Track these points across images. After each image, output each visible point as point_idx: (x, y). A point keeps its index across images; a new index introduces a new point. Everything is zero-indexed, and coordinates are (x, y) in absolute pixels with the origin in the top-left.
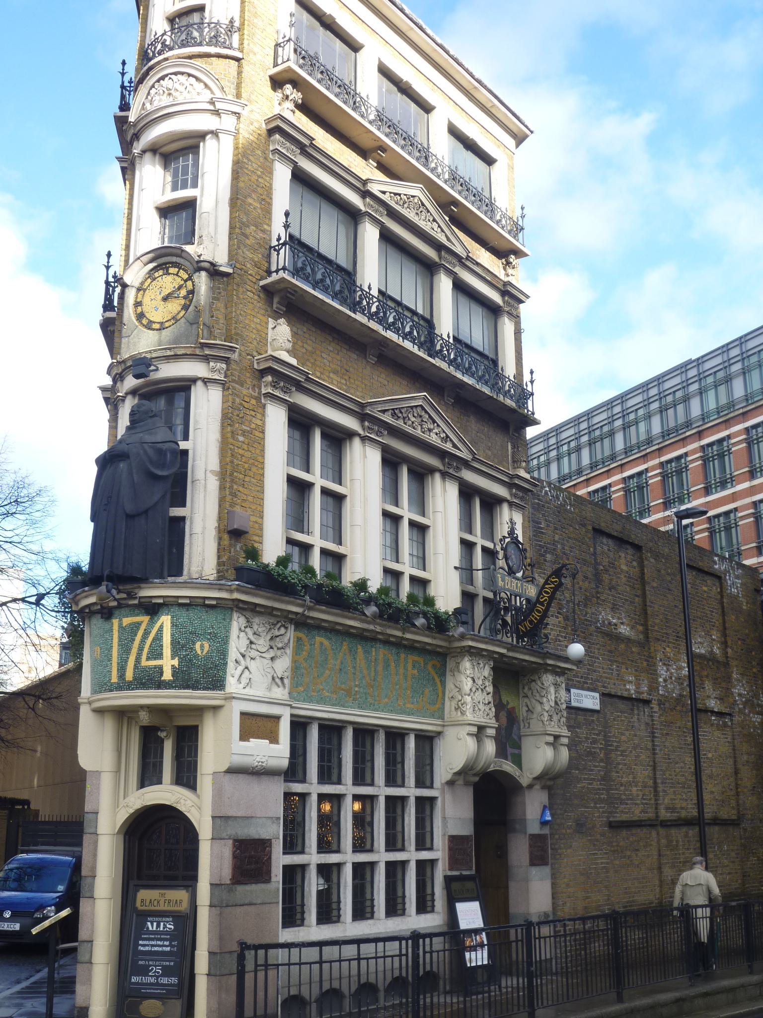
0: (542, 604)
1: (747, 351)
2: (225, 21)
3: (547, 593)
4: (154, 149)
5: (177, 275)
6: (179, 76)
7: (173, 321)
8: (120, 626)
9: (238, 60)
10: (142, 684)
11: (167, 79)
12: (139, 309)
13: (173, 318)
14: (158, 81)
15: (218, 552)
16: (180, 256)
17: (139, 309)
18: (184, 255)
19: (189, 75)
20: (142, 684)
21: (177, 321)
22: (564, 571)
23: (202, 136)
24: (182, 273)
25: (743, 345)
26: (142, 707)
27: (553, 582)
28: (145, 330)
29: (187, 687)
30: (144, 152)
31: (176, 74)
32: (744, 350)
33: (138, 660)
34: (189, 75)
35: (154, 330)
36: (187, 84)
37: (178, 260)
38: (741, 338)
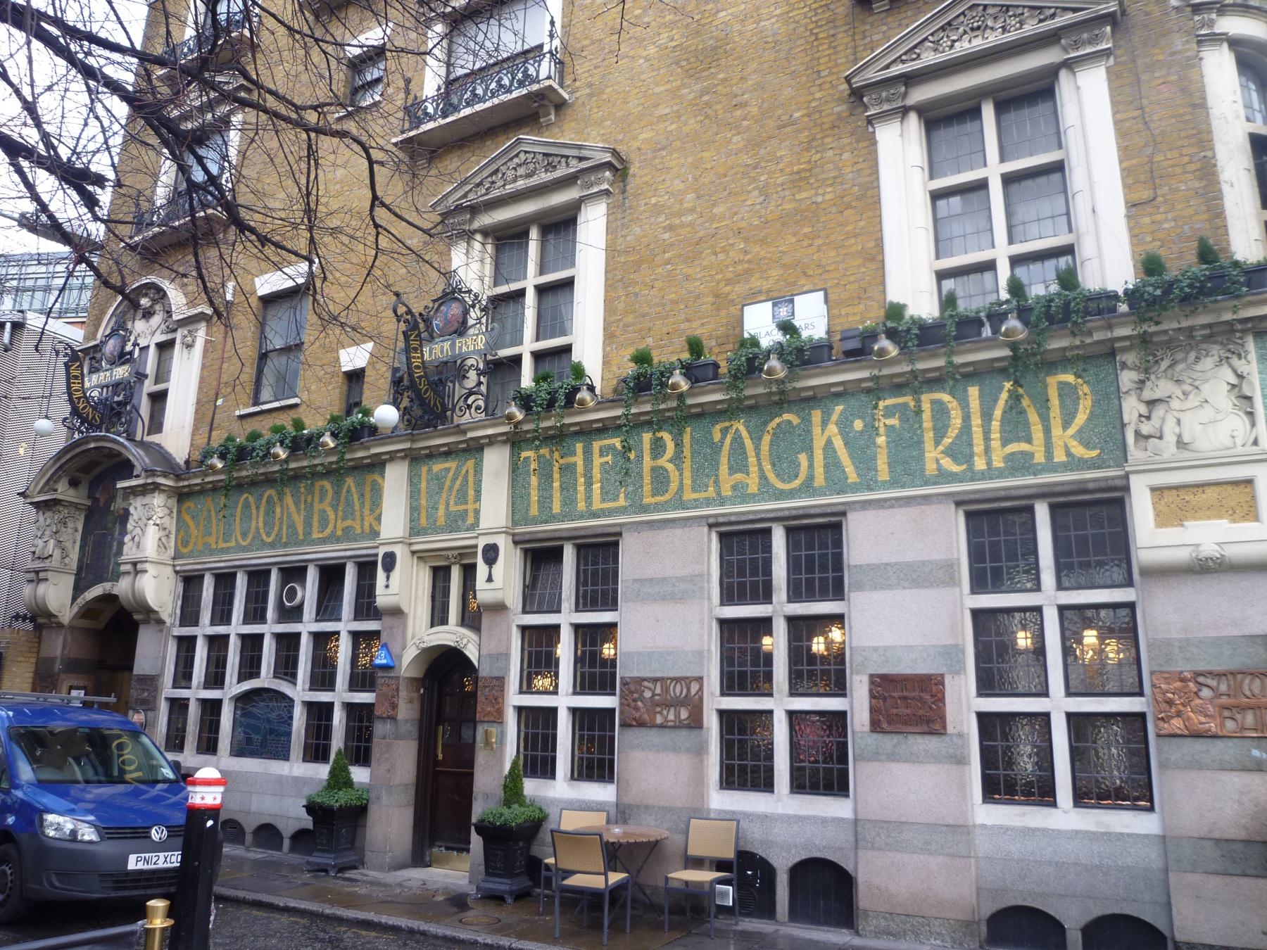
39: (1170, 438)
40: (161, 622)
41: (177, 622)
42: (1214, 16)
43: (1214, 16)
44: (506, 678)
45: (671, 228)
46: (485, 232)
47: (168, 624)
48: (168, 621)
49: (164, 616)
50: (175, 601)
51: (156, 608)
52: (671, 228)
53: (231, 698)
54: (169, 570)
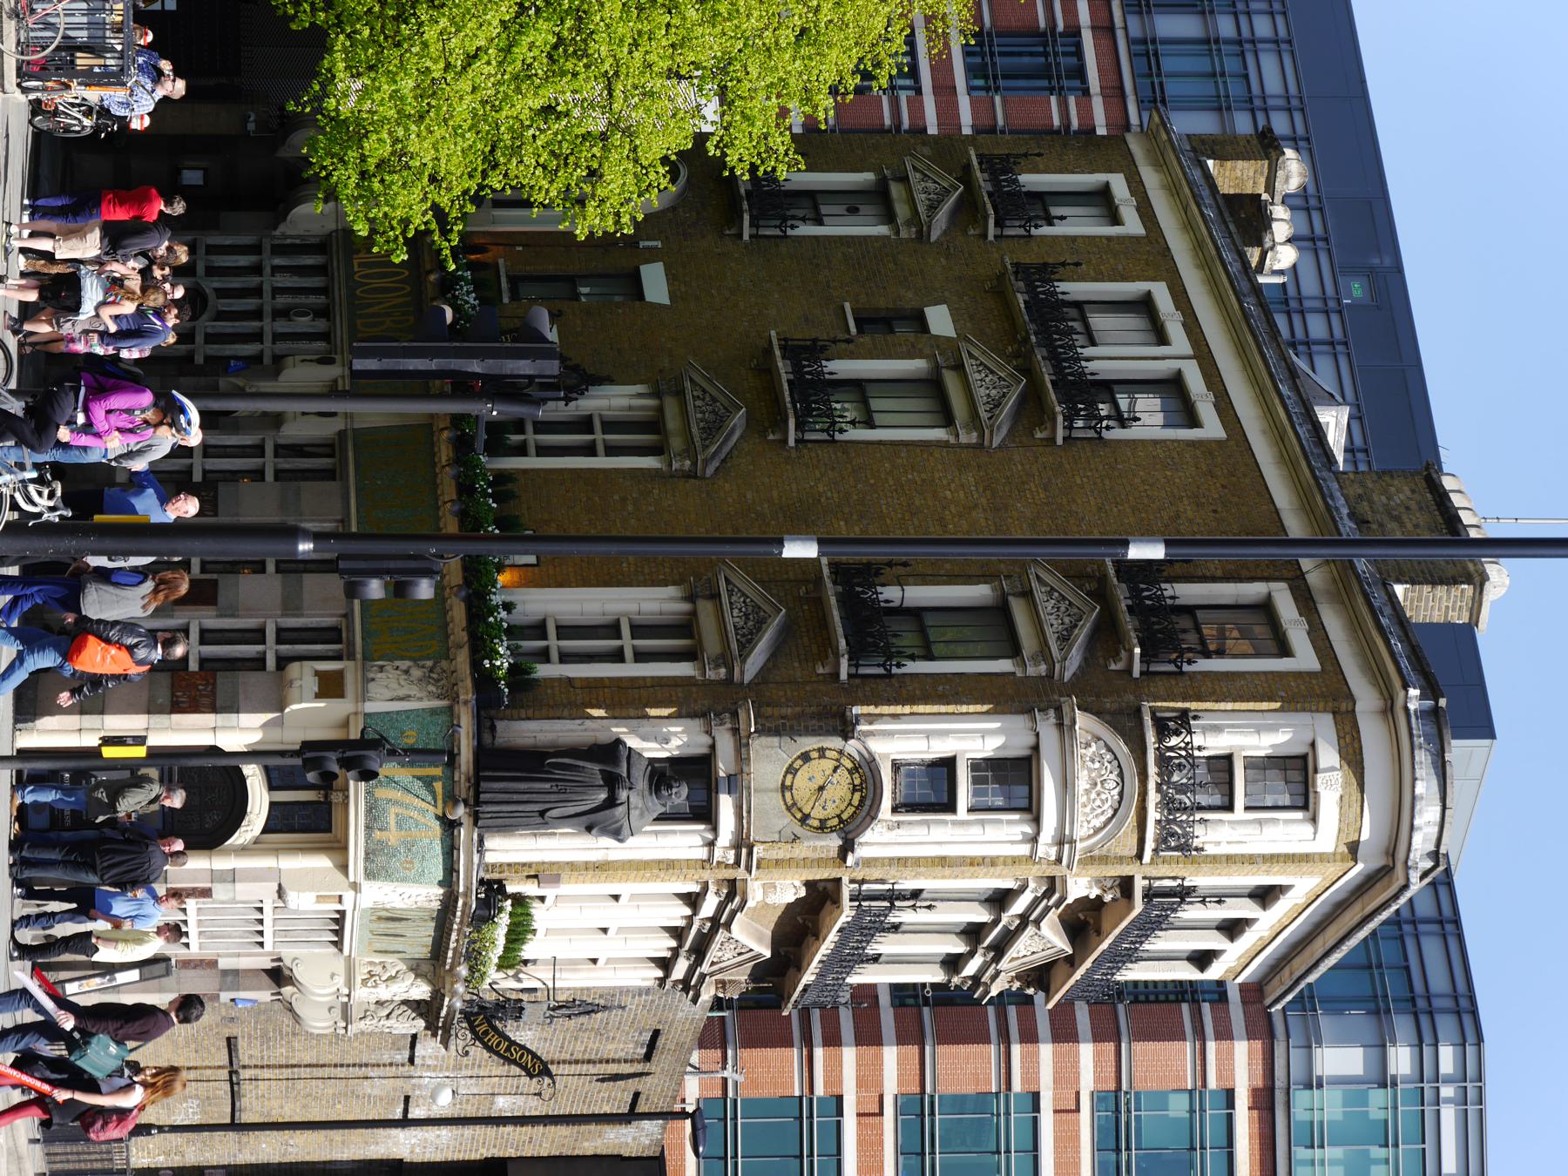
0: (508, 1049)
1: (1417, 937)
2: (1196, 843)
3: (522, 1055)
4: (1036, 748)
5: (850, 804)
6: (1116, 797)
7: (790, 802)
8: (434, 778)
9: (1140, 856)
10: (371, 809)
11: (1119, 780)
12: (814, 755)
13: (794, 804)
14: (1119, 766)
15: (516, 864)
16: (868, 814)
17: (814, 755)
18: (868, 818)
19: (1116, 811)
20: (371, 809)
21: (789, 809)
22: (547, 1080)
23: (1037, 820)
24: (851, 810)
25: (1435, 928)
26: (347, 797)
27: (534, 1066)
28: (787, 765)
29: (367, 854)
30: (1037, 735)
31: (1121, 794)
32: (1422, 927)
33: (396, 803)
34: (1116, 811)
35: (785, 777)
36: (1106, 806)
37: (866, 808)
38: (1457, 922)
39: (379, 675)
40: (275, 229)
41: (277, 242)
42: (729, 725)
43: (729, 725)
44: (217, 432)
45: (624, 500)
46: (660, 409)
47: (274, 233)
48: (277, 233)
49: (282, 229)
50: (299, 237)
51: (289, 218)
52: (624, 500)
53: (197, 283)
54: (333, 227)
